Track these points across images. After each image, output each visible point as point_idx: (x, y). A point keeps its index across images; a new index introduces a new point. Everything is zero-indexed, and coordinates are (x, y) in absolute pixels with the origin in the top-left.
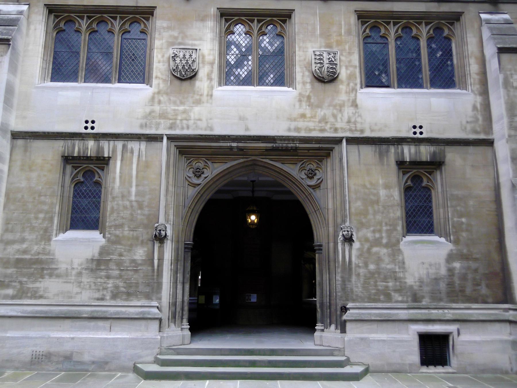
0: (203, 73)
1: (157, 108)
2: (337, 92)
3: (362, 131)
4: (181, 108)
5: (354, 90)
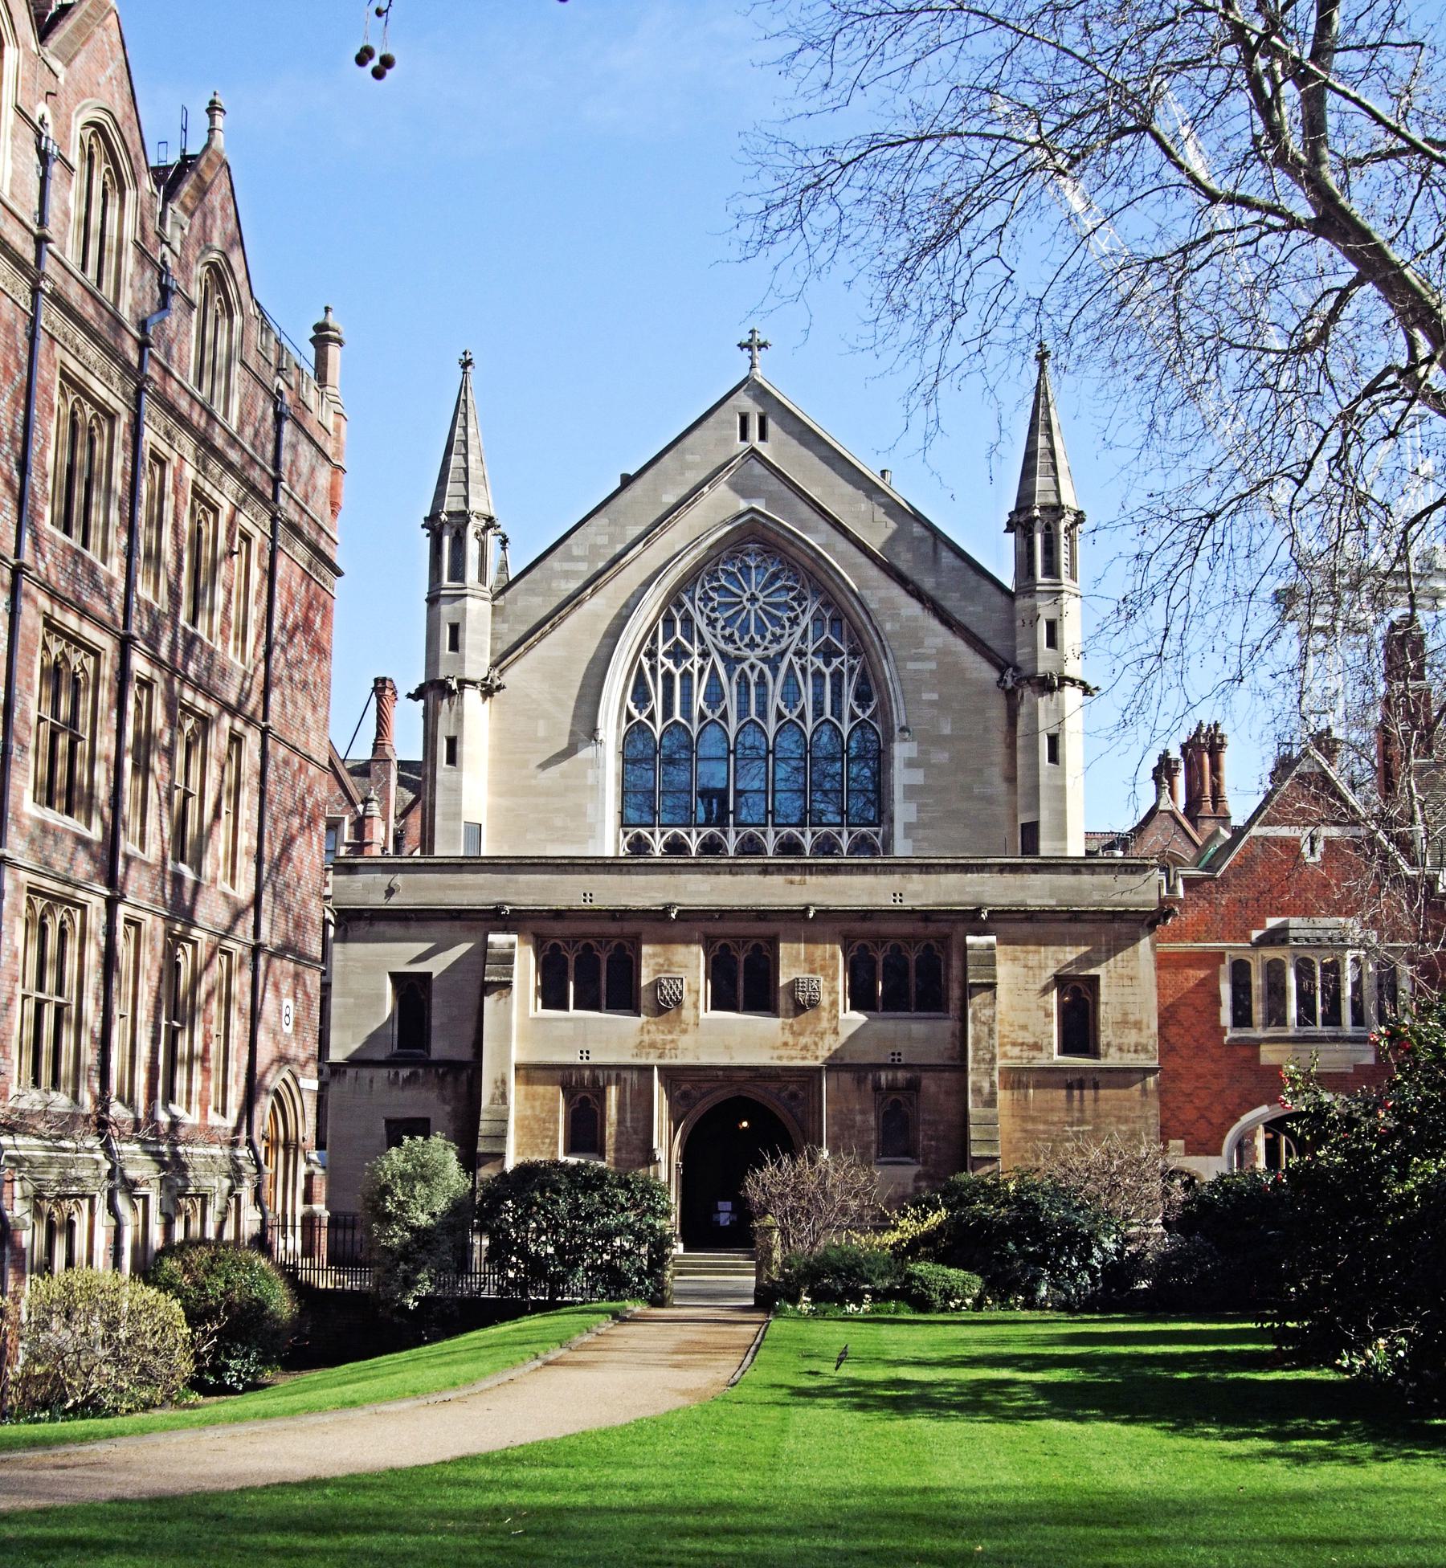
2: (819, 1019)
4: (669, 1037)
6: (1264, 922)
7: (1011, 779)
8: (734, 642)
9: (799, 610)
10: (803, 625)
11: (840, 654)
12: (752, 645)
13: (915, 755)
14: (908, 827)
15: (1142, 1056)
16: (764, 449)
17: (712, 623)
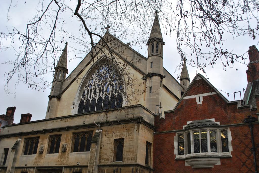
3: (68, 164)
4: (39, 160)
5: (69, 154)
6: (186, 123)
7: (145, 100)
15: (133, 161)
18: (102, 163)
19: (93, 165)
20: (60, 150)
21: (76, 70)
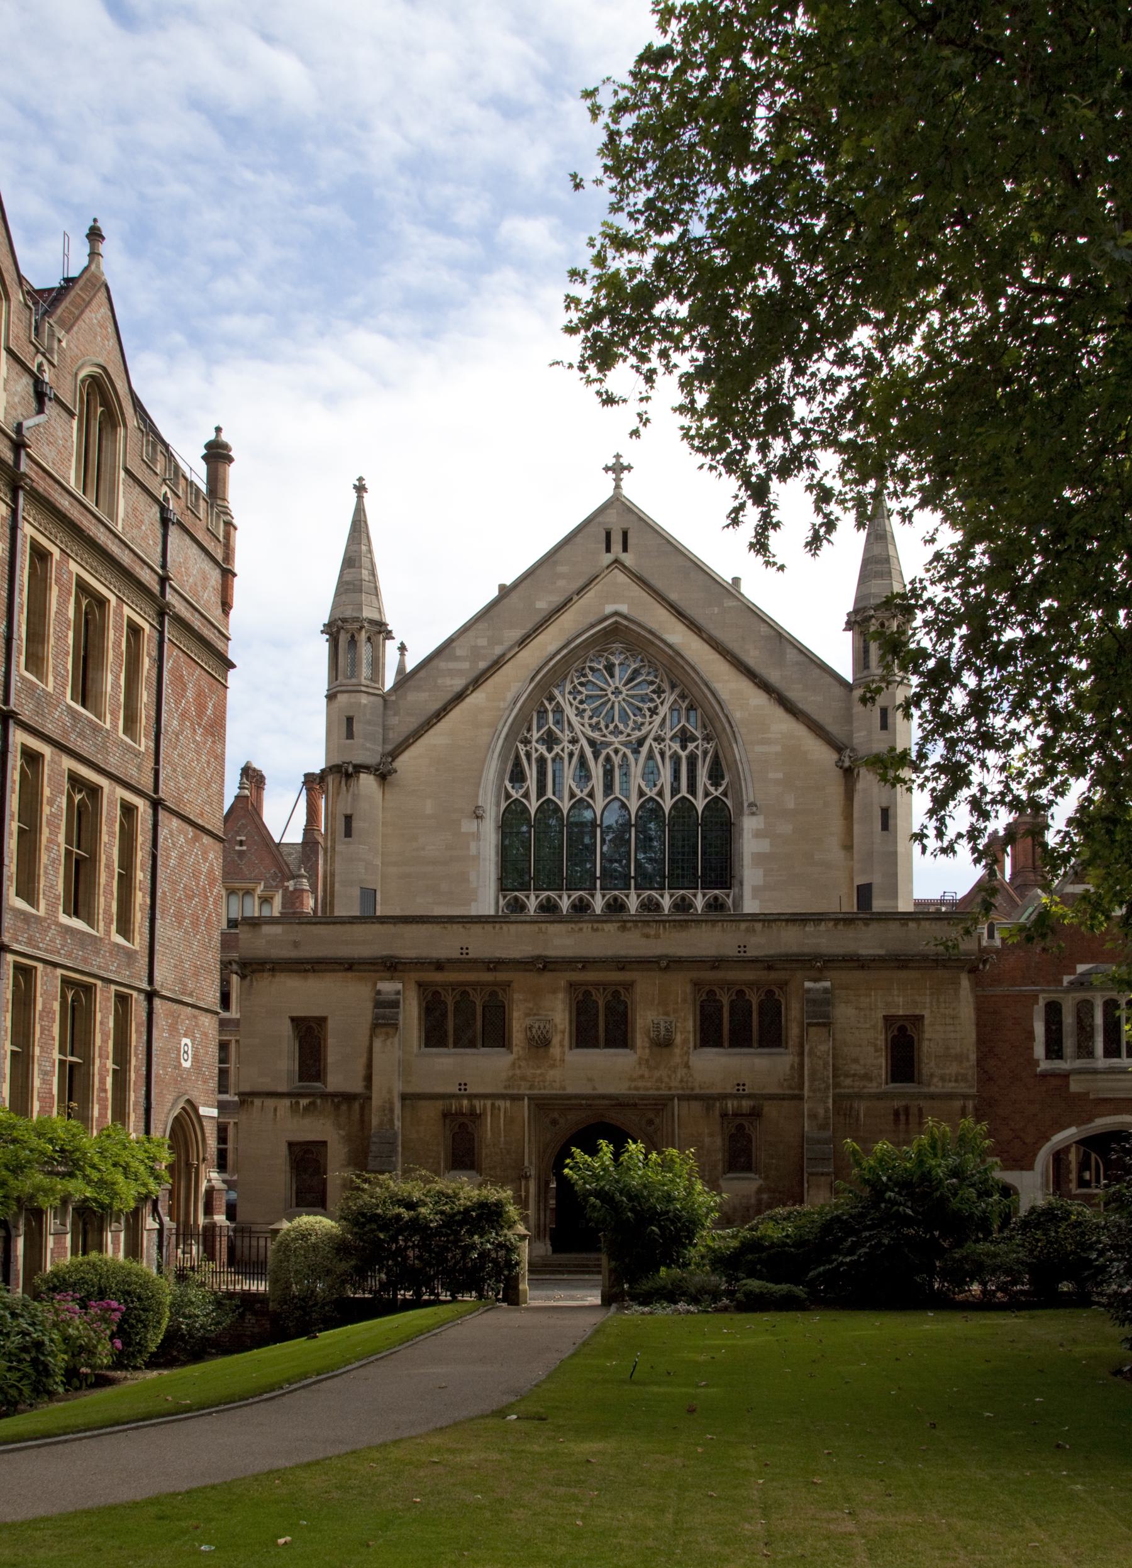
0: (556, 1040)
1: (518, 1072)
3: (692, 1089)
4: (539, 1072)
5: (687, 1053)
6: (1075, 968)
7: (848, 847)
8: (600, 730)
9: (658, 701)
10: (662, 715)
11: (694, 739)
12: (617, 732)
13: (762, 826)
14: (756, 890)
15: (963, 1084)
16: (628, 559)
17: (580, 713)
18: (845, 1087)
19: (827, 1097)
20: (640, 1039)
21: (460, 650)
